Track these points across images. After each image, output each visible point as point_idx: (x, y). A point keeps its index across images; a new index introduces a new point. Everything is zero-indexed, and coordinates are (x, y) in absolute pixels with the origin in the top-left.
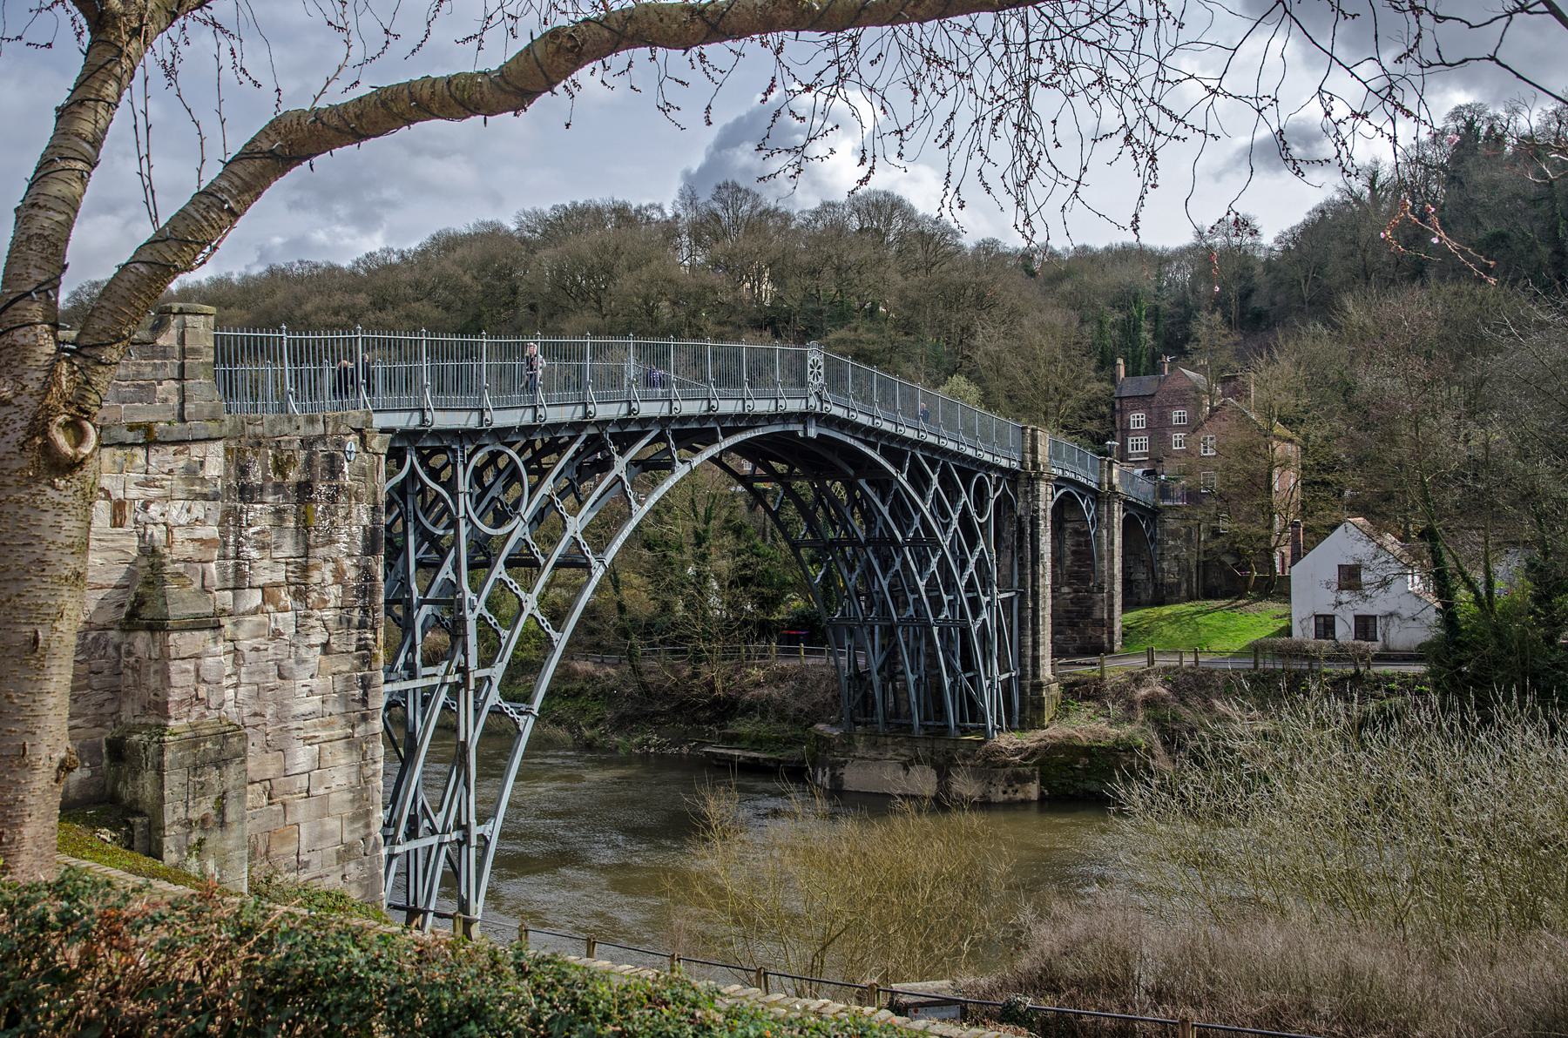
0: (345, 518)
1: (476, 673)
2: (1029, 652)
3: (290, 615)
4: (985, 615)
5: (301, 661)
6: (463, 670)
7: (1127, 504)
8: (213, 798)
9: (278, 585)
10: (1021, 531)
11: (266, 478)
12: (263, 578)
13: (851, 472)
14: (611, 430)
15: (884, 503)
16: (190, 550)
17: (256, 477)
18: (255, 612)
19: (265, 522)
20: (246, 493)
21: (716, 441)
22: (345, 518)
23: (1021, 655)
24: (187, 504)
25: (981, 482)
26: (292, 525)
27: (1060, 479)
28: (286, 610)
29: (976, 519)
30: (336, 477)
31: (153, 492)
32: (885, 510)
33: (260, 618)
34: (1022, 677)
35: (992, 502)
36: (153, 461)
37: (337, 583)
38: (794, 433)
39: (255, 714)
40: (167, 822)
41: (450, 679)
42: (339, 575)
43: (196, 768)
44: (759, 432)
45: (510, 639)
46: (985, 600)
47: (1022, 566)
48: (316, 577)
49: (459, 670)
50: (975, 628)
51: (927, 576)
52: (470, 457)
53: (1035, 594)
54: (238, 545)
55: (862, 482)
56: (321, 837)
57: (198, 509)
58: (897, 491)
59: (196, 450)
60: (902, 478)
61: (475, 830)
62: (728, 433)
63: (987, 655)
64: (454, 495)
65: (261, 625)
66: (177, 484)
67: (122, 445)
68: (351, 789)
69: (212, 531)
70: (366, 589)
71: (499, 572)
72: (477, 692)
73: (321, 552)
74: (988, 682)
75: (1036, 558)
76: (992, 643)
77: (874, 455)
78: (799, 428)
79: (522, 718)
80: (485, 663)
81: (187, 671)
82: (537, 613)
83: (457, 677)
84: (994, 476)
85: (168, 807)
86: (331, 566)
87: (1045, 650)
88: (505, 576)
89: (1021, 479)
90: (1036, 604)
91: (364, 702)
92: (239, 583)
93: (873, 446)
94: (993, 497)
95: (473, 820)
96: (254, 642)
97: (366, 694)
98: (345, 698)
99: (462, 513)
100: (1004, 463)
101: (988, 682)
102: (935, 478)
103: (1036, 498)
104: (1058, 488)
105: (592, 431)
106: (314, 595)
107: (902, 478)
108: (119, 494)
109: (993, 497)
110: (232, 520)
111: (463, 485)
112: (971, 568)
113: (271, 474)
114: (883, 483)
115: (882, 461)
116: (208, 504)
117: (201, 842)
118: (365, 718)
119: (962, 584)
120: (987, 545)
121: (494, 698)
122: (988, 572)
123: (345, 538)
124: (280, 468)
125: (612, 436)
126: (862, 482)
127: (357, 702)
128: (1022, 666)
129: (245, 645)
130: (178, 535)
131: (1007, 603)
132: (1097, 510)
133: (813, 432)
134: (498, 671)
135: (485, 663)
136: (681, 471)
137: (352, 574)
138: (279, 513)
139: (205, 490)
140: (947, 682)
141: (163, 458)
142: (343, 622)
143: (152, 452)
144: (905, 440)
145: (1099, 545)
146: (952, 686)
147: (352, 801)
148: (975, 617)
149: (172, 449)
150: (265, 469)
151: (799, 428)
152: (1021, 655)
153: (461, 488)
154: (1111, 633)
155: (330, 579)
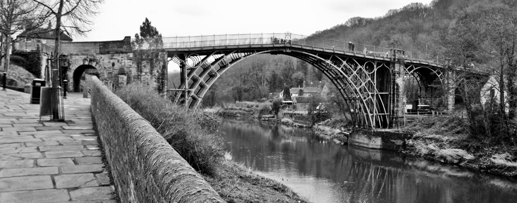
12: (145, 71)
17: (144, 57)
19: (145, 64)
20: (143, 60)
35: (375, 70)
42: (158, 72)
46: (370, 93)
48: (154, 71)
57: (129, 61)
59: (128, 54)
62: (258, 51)
66: (126, 58)
74: (372, 115)
77: (316, 56)
101: (372, 115)
115: (319, 57)
124: (148, 56)
129: (142, 80)
132: (443, 74)
133: (288, 51)
137: (160, 71)
141: (124, 55)
144: (328, 53)
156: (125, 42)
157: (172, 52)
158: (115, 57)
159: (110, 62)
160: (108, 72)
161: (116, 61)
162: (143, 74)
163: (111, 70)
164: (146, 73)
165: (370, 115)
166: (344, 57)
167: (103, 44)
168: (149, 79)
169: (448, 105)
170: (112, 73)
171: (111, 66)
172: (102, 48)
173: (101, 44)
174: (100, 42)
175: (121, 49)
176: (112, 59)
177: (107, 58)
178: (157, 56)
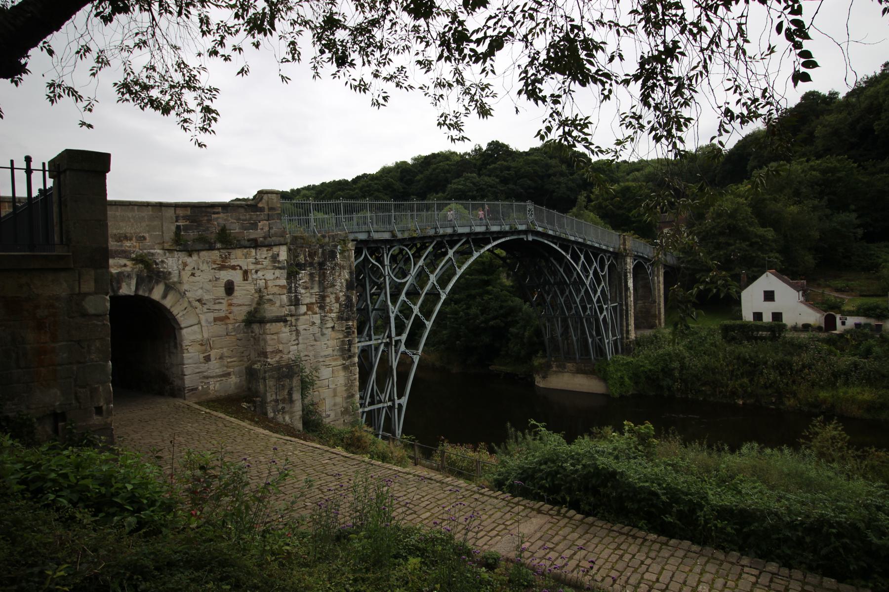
0: (339, 276)
1: (396, 339)
2: (625, 329)
3: (318, 316)
4: (605, 313)
5: (323, 334)
6: (390, 336)
7: (665, 266)
8: (287, 391)
9: (312, 304)
10: (620, 278)
11: (306, 260)
12: (307, 300)
13: (547, 255)
14: (447, 239)
15: (561, 267)
16: (276, 290)
18: (305, 314)
19: (306, 279)
21: (489, 243)
22: (339, 276)
23: (622, 330)
24: (273, 271)
25: (602, 257)
26: (317, 279)
27: (636, 256)
28: (316, 313)
29: (601, 273)
30: (334, 260)
31: (259, 267)
32: (562, 270)
33: (306, 317)
34: (622, 338)
35: (607, 267)
36: (258, 254)
37: (336, 302)
38: (523, 239)
39: (306, 356)
40: (268, 400)
41: (384, 341)
42: (337, 299)
43: (279, 379)
44: (508, 239)
45: (409, 324)
46: (605, 307)
47: (621, 293)
48: (328, 300)
49: (388, 337)
50: (601, 318)
51: (580, 296)
52: (389, 251)
53: (627, 305)
54: (296, 287)
55: (552, 259)
56: (335, 405)
57: (278, 273)
58: (566, 263)
59: (275, 250)
60: (569, 257)
61: (397, 402)
62: (494, 240)
63: (607, 330)
64: (383, 266)
65: (307, 320)
67: (246, 247)
68: (346, 385)
69: (283, 282)
70: (349, 304)
71: (403, 297)
72: (396, 346)
73: (330, 290)
75: (627, 289)
76: (608, 325)
78: (524, 237)
79: (415, 356)
80: (399, 334)
81: (274, 339)
82: (419, 314)
83: (388, 340)
84: (608, 255)
85: (268, 395)
86: (334, 296)
87: (632, 327)
88: (405, 299)
89: (618, 256)
90: (627, 308)
91: (349, 350)
92: (296, 302)
93: (556, 244)
94: (607, 264)
95: (396, 398)
96: (304, 327)
97: (350, 347)
98: (342, 350)
99: (387, 273)
100: (611, 250)
102: (582, 257)
103: (626, 264)
104: (635, 260)
105: (439, 239)
106: (328, 308)
107: (569, 257)
108: (244, 268)
109: (607, 264)
110: (292, 276)
111: (387, 262)
112: (599, 293)
113: (308, 259)
114: (561, 259)
115: (560, 250)
116: (281, 271)
117: (283, 408)
118: (350, 357)
119: (595, 300)
120: (605, 284)
121: (403, 348)
122: (606, 295)
123: (339, 284)
124: (312, 255)
125: (447, 241)
126: (552, 259)
127: (345, 351)
128: (622, 334)
129: (301, 328)
130: (270, 284)
131: (615, 308)
133: (530, 238)
134: (404, 337)
135: (399, 334)
136: (476, 255)
138: (311, 275)
139: (280, 265)
140: (590, 340)
142: (340, 318)
143: (258, 250)
145: (654, 284)
146: (592, 342)
147: (346, 390)
148: (601, 313)
149: (265, 249)
150: (305, 257)
151: (524, 237)
152: (622, 330)
153: (386, 263)
154: (660, 320)
155: (334, 301)
156: (262, 210)
157: (362, 241)
158: (233, 263)
159: (217, 279)
160: (211, 316)
161: (236, 277)
162: (303, 309)
163: (224, 307)
164: (309, 306)
165: (606, 341)
166: (582, 246)
167: (188, 212)
168: (318, 322)
169: (660, 313)
170: (227, 318)
171: (221, 292)
172: (186, 228)
173: (180, 212)
174: (176, 206)
175: (252, 234)
176: (222, 268)
177: (204, 267)
178: (333, 255)
